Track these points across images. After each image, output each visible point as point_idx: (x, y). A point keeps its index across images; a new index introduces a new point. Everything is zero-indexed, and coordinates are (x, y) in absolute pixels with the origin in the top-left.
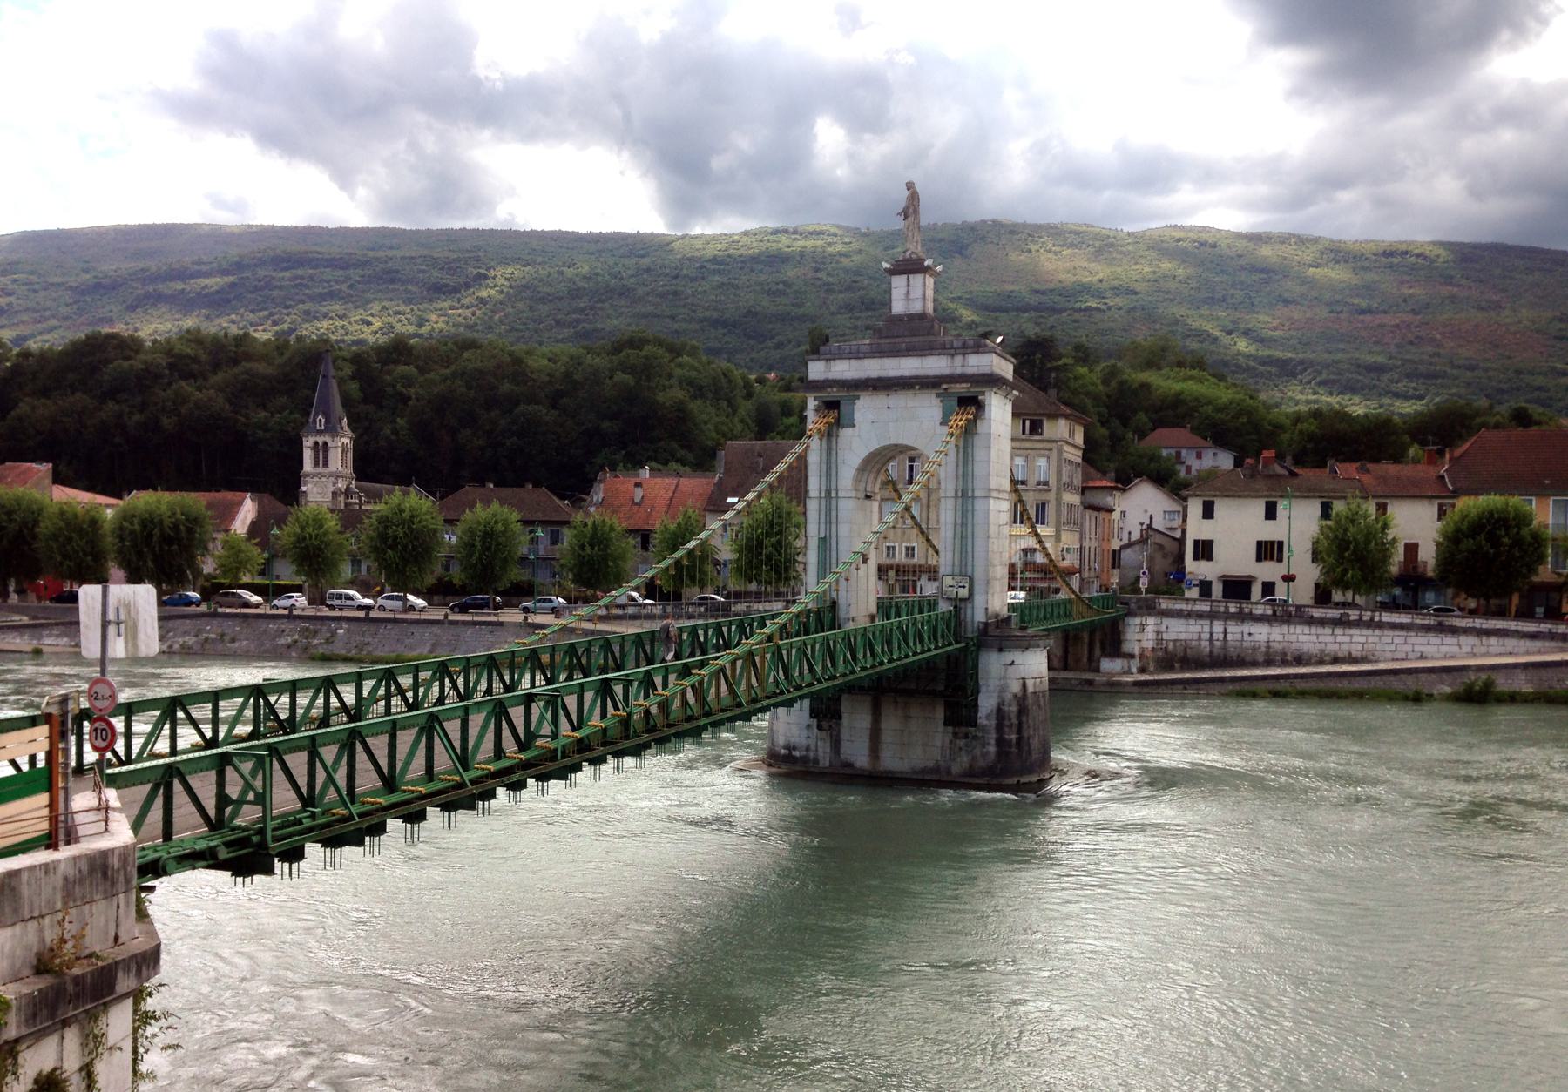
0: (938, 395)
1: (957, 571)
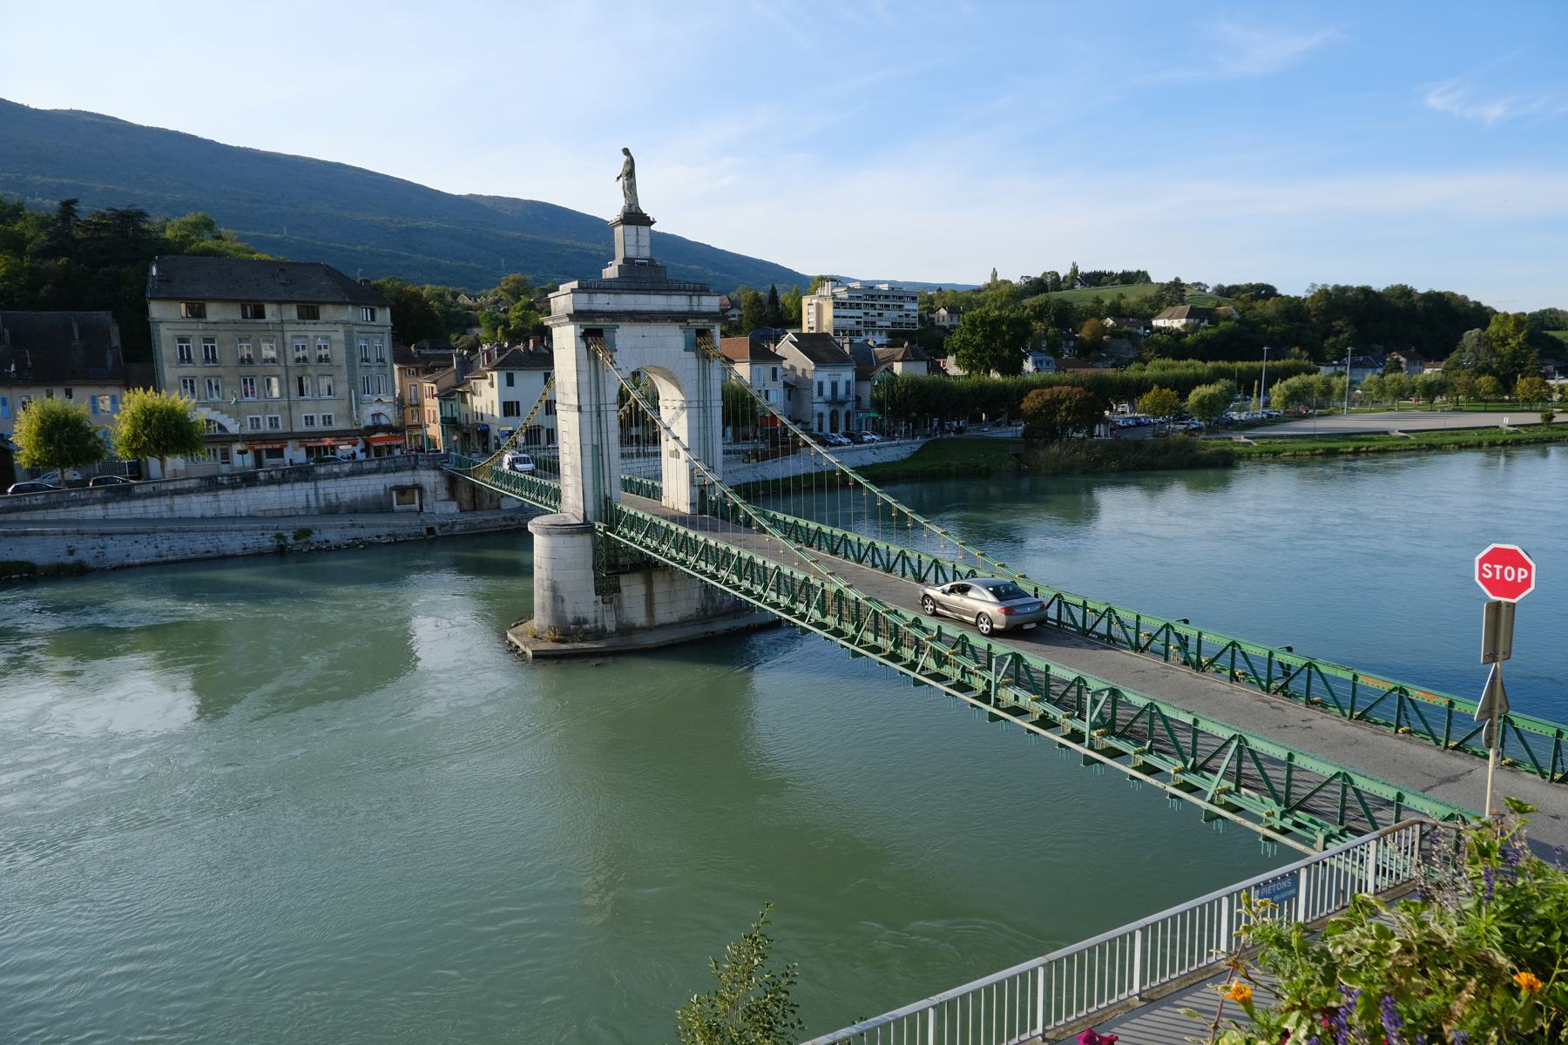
0: (681, 327)
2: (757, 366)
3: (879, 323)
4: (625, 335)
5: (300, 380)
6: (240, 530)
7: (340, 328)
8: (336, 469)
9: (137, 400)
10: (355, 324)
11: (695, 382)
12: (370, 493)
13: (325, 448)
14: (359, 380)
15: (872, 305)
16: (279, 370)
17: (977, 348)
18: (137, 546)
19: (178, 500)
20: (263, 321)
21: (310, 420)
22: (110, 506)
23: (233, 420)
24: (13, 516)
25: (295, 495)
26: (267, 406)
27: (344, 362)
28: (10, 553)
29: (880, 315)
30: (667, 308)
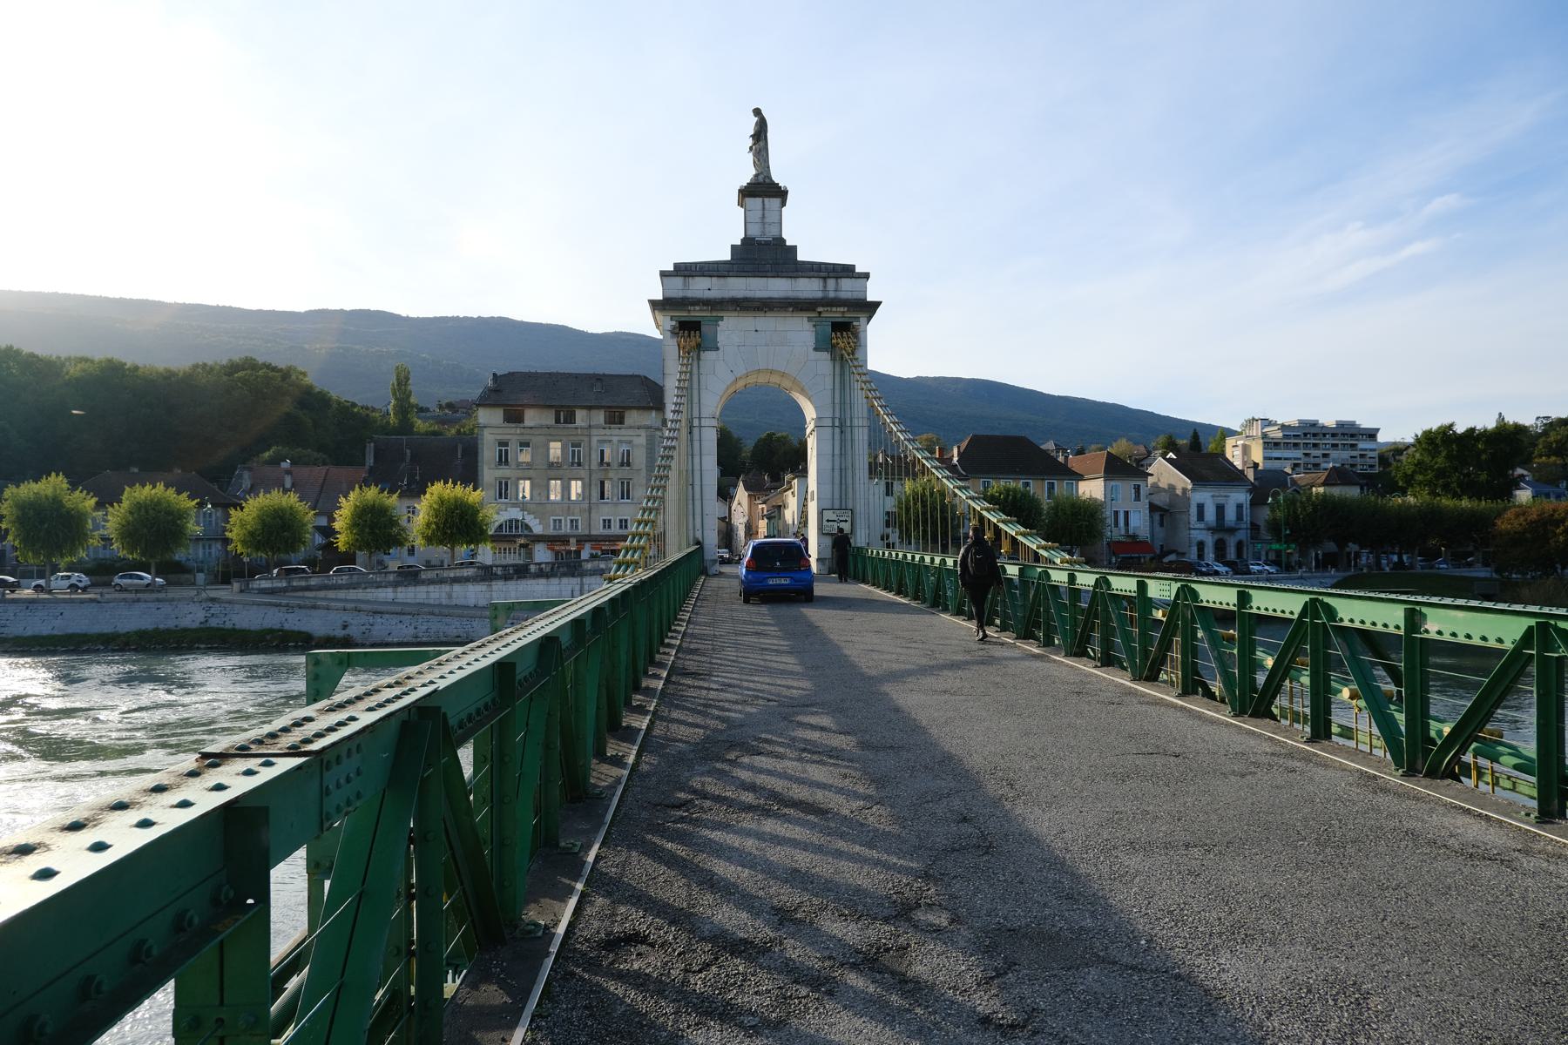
0: (810, 319)
1: (837, 506)
2: (1113, 483)
3: (1324, 465)
5: (602, 484)
7: (643, 432)
11: (829, 393)
15: (1315, 445)
16: (583, 473)
17: (1441, 473)
18: (400, 626)
19: (457, 588)
20: (573, 425)
22: (399, 589)
24: (322, 594)
26: (569, 507)
27: (644, 466)
28: (297, 623)
29: (1325, 456)
30: (791, 294)
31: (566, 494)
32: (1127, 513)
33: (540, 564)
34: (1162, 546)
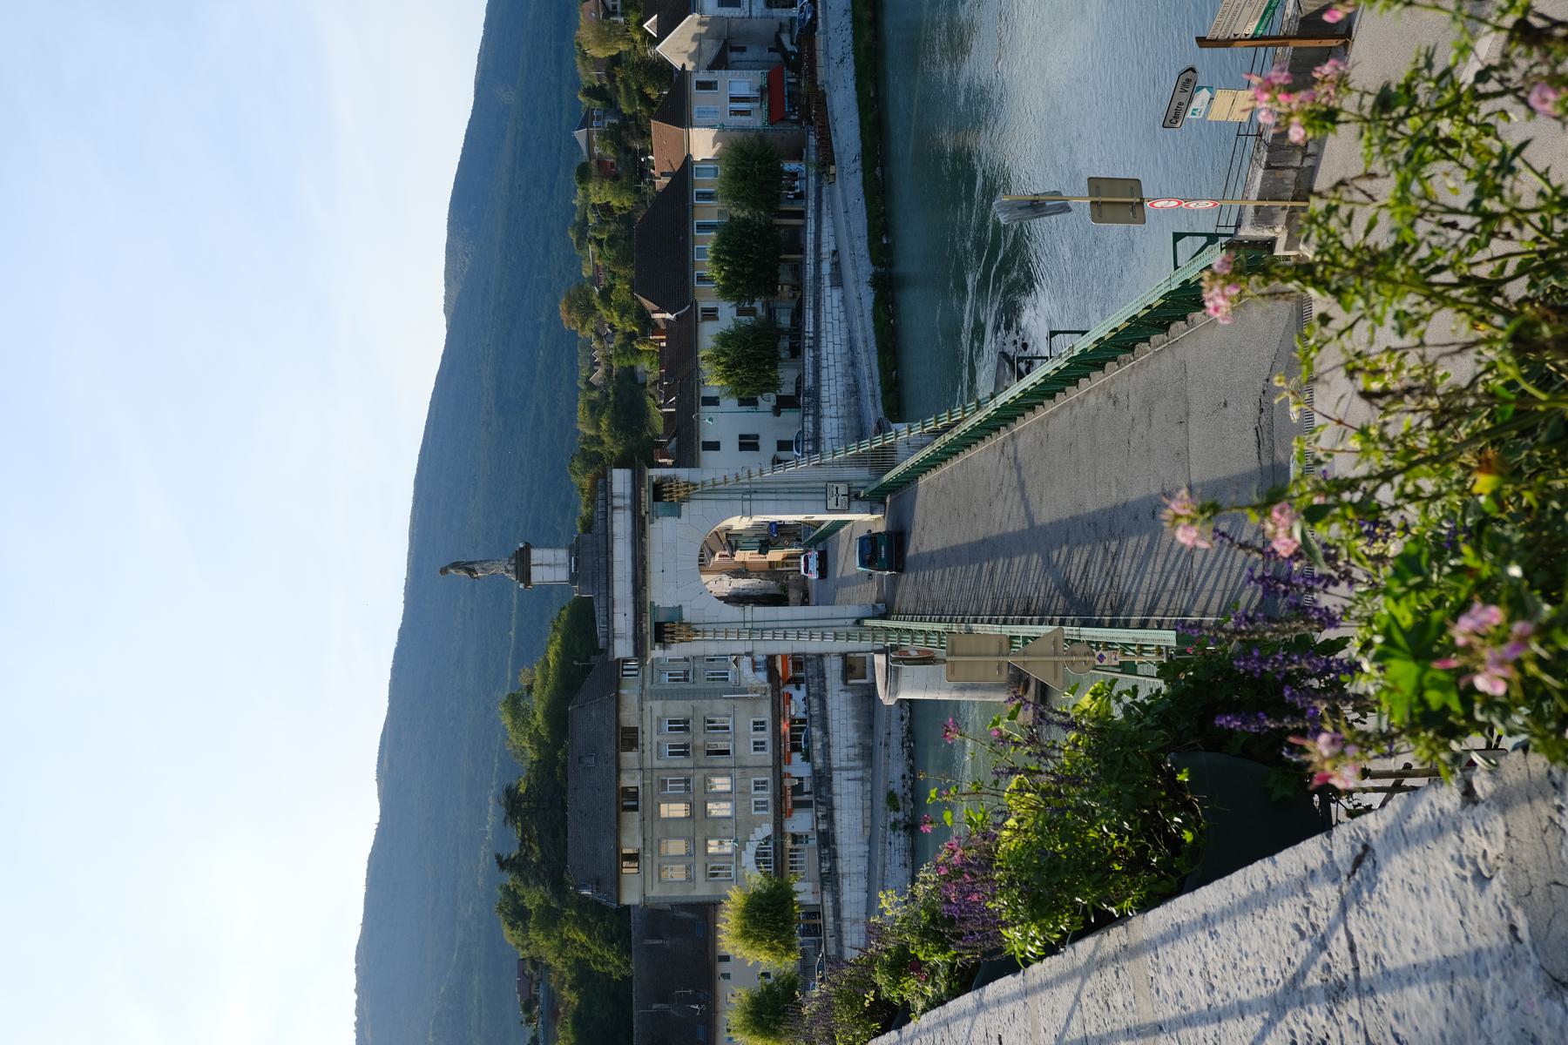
0: (651, 522)
1: (823, 497)
2: (695, 117)
4: (662, 595)
5: (709, 753)
6: (884, 866)
7: (648, 704)
8: (818, 745)
9: (729, 937)
10: (643, 687)
11: (719, 503)
12: (850, 709)
13: (792, 730)
14: (710, 685)
16: (698, 776)
19: (846, 914)
21: (759, 746)
23: (757, 829)
25: (848, 797)
27: (689, 703)
30: (628, 540)
31: (723, 796)
32: (733, 99)
33: (817, 818)
34: (770, 50)
